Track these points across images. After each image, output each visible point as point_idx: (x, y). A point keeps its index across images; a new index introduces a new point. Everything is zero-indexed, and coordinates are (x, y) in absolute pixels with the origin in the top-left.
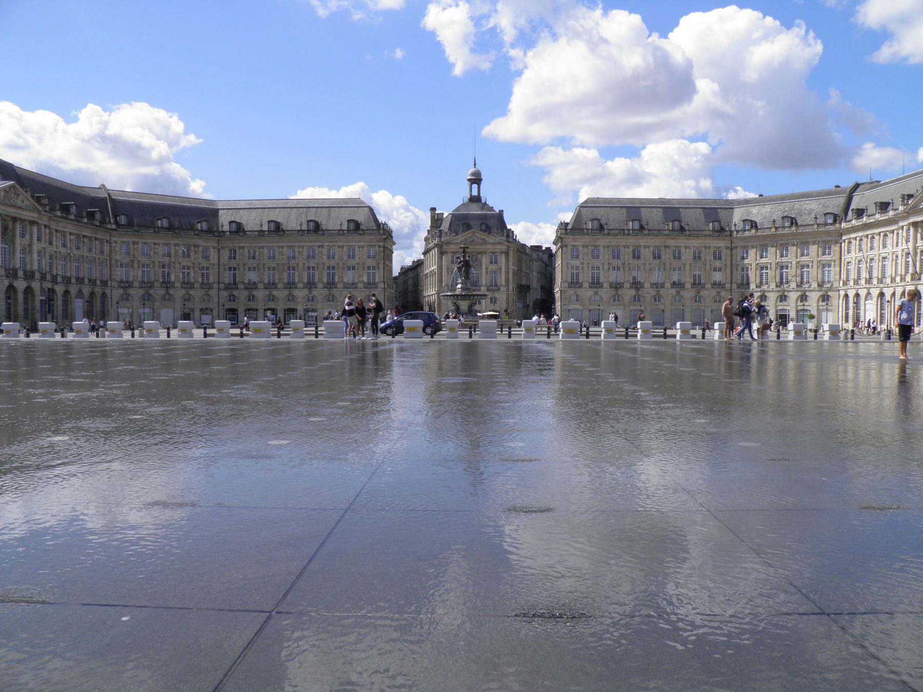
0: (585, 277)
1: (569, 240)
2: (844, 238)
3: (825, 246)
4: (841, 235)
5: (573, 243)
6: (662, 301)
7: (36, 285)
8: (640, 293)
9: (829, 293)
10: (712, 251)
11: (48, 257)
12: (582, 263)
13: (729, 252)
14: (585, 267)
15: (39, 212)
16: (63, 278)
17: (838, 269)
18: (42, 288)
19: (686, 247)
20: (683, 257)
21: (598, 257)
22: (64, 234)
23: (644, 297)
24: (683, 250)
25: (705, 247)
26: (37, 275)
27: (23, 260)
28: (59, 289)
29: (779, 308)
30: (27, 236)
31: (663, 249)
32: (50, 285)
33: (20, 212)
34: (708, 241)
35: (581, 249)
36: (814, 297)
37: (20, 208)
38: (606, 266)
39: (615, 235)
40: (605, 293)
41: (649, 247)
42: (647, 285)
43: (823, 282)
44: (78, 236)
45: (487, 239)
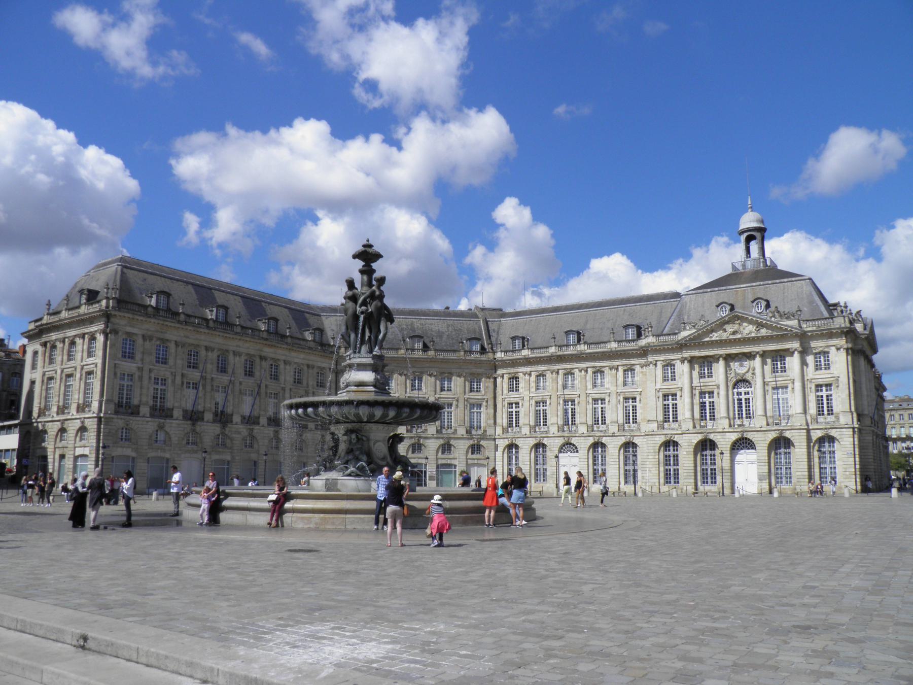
0: (143, 396)
1: (122, 321)
2: (500, 372)
3: (473, 379)
4: (495, 369)
5: (129, 329)
6: (256, 446)
8: (227, 429)
9: (482, 443)
10: (316, 370)
12: (140, 369)
19: (285, 362)
20: (282, 378)
21: (165, 362)
23: (232, 439)
24: (282, 366)
25: (308, 366)
29: (440, 462)
31: (258, 360)
34: (312, 357)
35: (140, 341)
36: (461, 447)
38: (178, 379)
39: (193, 325)
40: (176, 427)
41: (240, 354)
42: (237, 419)
43: (472, 427)
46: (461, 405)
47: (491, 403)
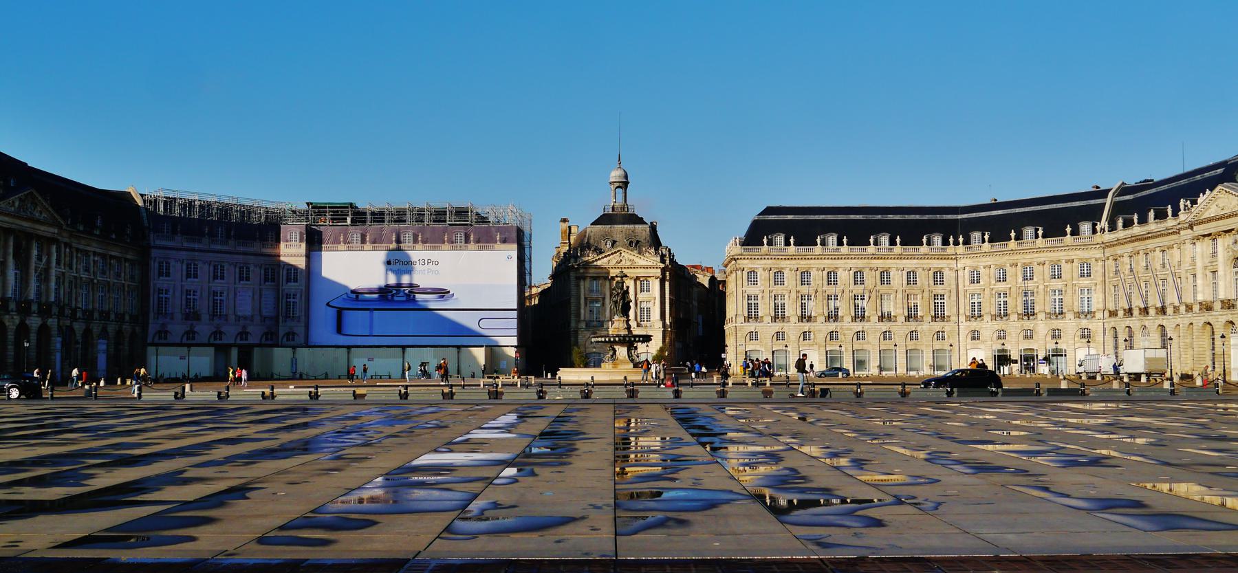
7: (52, 322)
11: (67, 284)
13: (953, 274)
14: (766, 295)
15: (60, 227)
16: (84, 312)
17: (1101, 296)
18: (60, 328)
22: (86, 253)
26: (55, 310)
27: (39, 293)
28: (78, 327)
30: (44, 260)
32: (68, 323)
33: (37, 226)
37: (38, 222)
38: (793, 295)
44: (103, 256)
45: (637, 260)
46: (1070, 291)
47: (1100, 287)
